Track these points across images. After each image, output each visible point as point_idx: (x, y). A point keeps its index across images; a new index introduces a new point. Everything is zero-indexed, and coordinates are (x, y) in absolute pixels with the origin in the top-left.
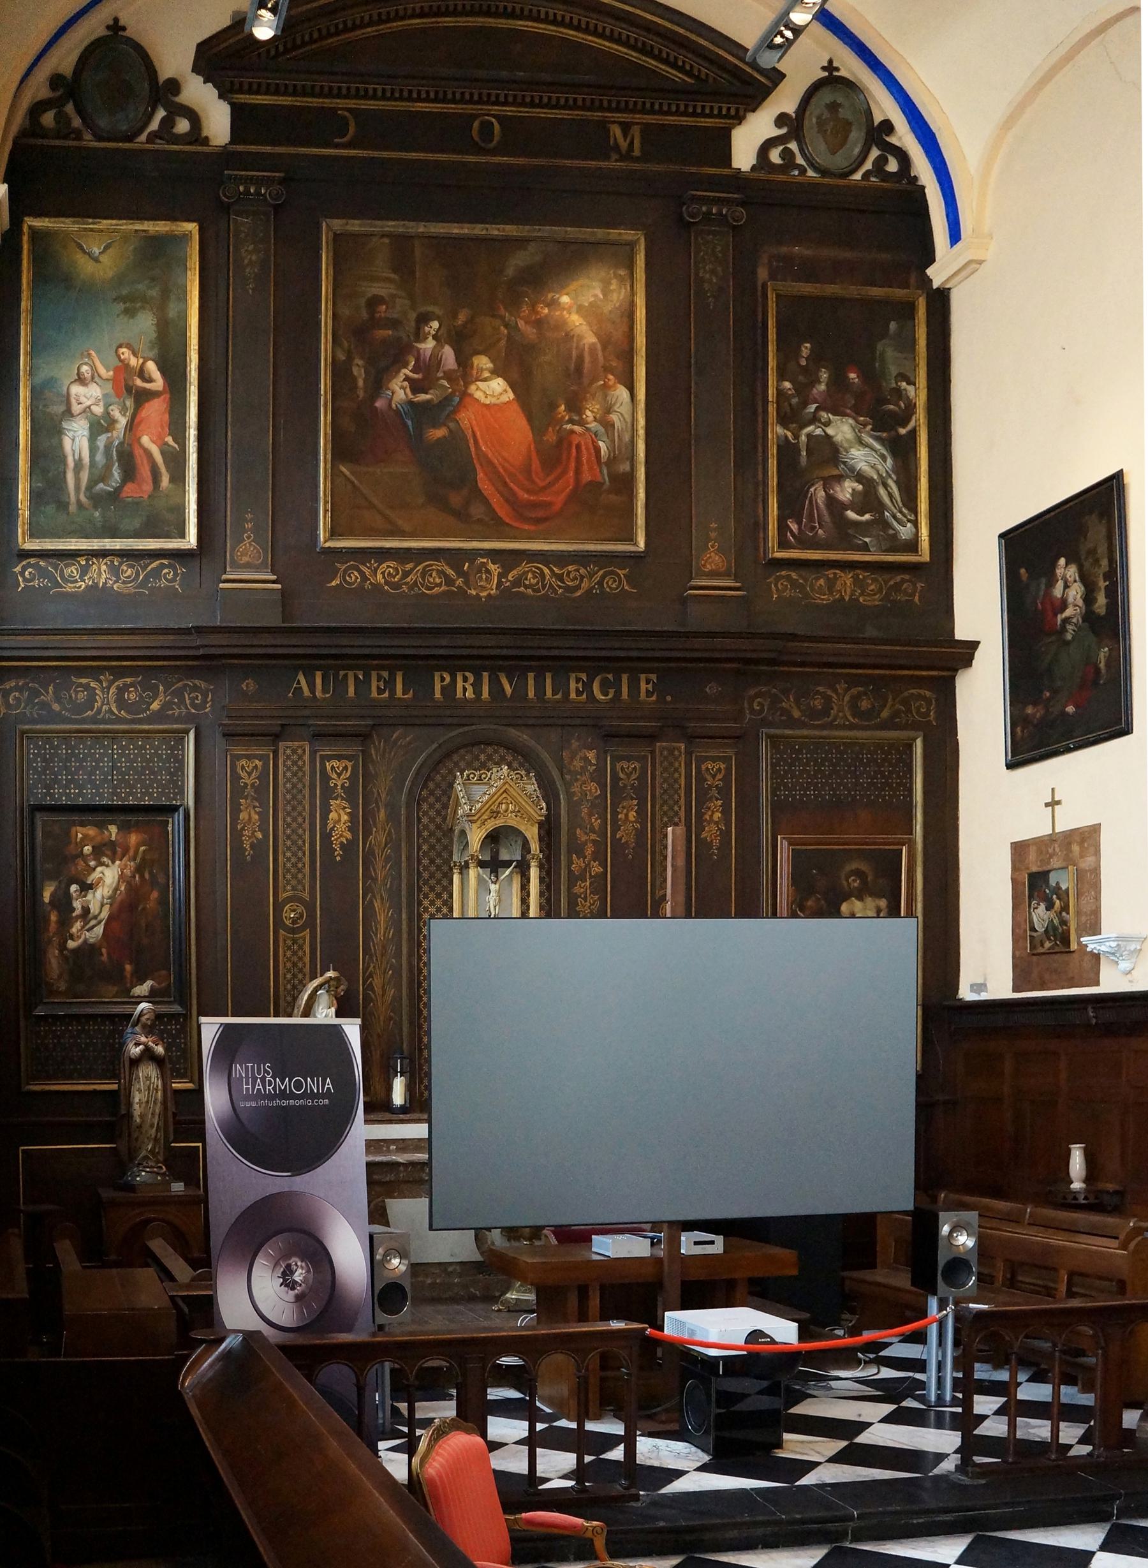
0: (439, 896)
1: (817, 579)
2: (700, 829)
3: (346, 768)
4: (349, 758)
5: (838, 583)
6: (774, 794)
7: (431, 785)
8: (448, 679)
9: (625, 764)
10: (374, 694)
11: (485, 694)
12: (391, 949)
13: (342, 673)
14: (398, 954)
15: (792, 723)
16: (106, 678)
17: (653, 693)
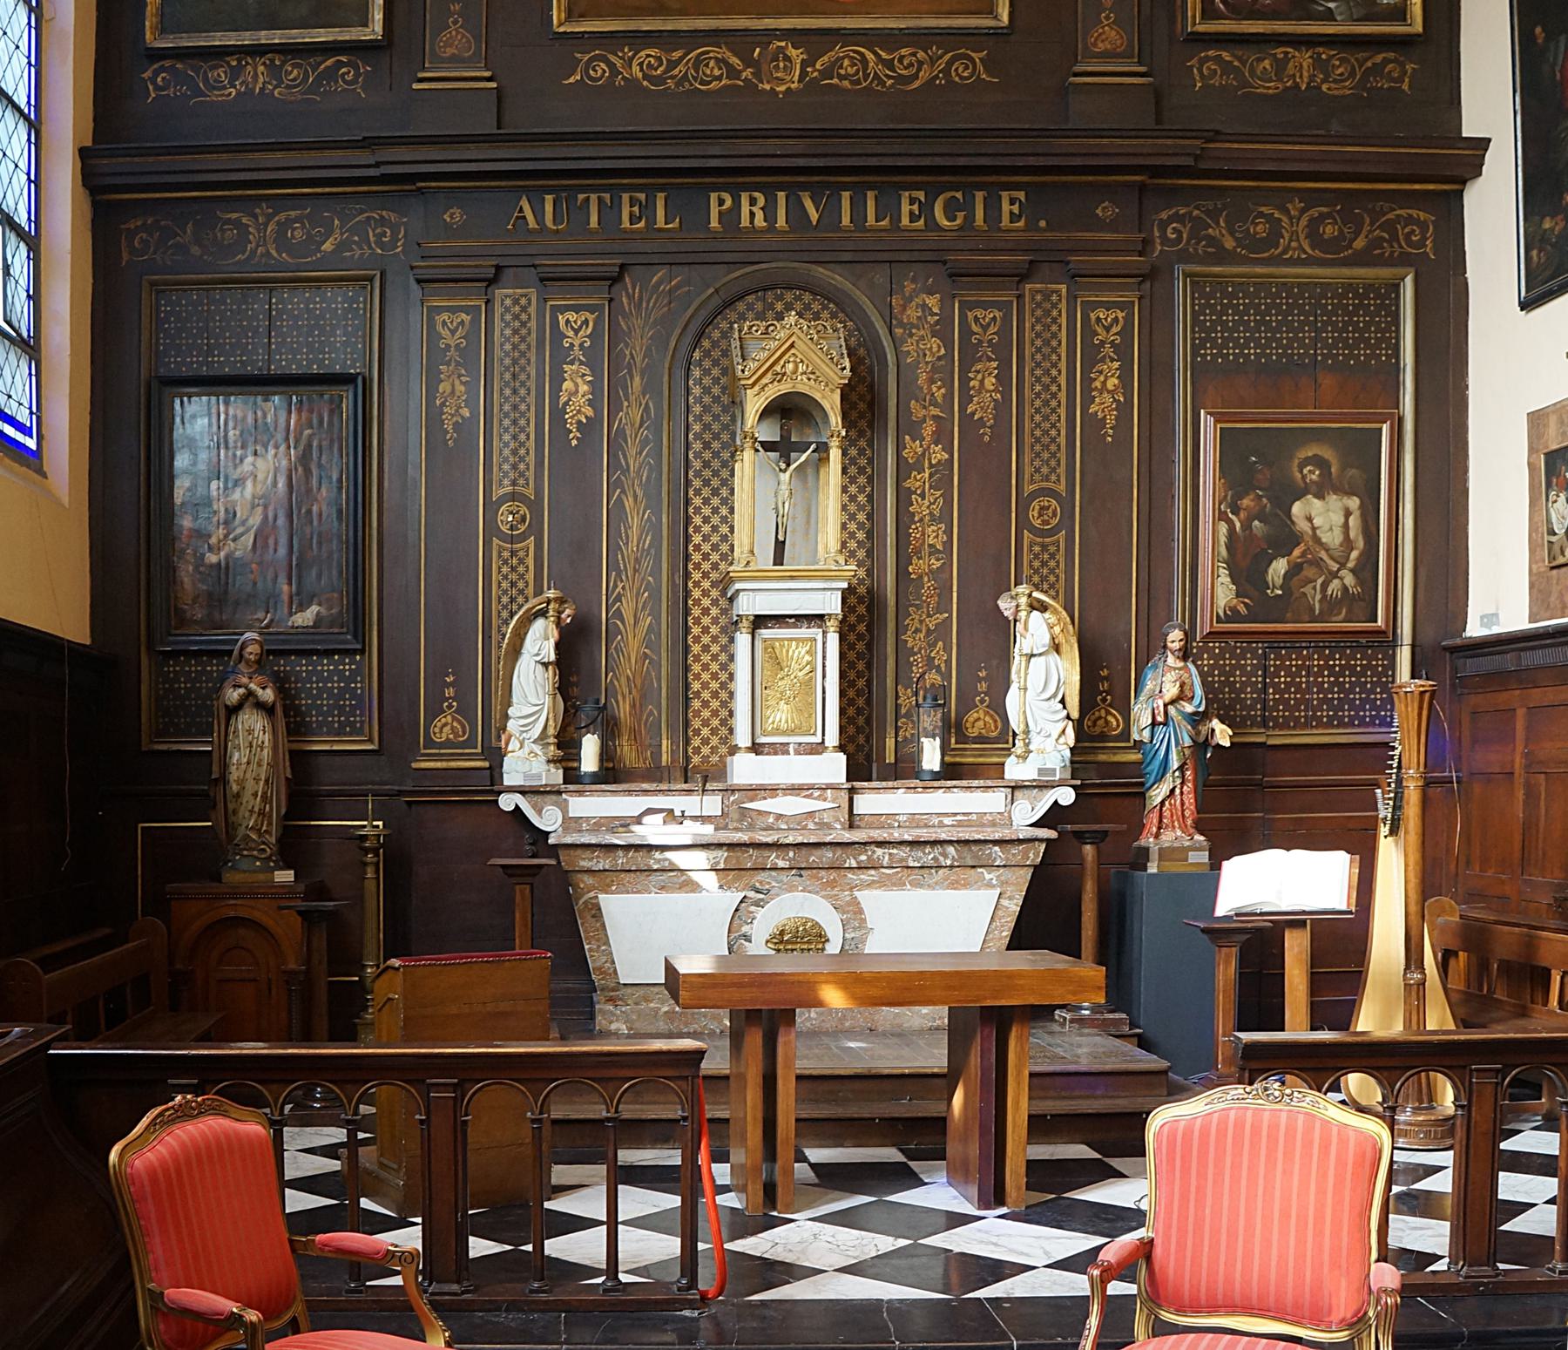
0: (715, 492)
1: (1260, 60)
2: (1088, 400)
3: (586, 322)
4: (591, 309)
5: (1291, 65)
6: (1194, 355)
7: (706, 343)
8: (728, 203)
9: (979, 313)
10: (626, 224)
11: (781, 221)
12: (647, 564)
13: (581, 197)
14: (656, 572)
15: (1222, 256)
16: (262, 210)
17: (1020, 216)
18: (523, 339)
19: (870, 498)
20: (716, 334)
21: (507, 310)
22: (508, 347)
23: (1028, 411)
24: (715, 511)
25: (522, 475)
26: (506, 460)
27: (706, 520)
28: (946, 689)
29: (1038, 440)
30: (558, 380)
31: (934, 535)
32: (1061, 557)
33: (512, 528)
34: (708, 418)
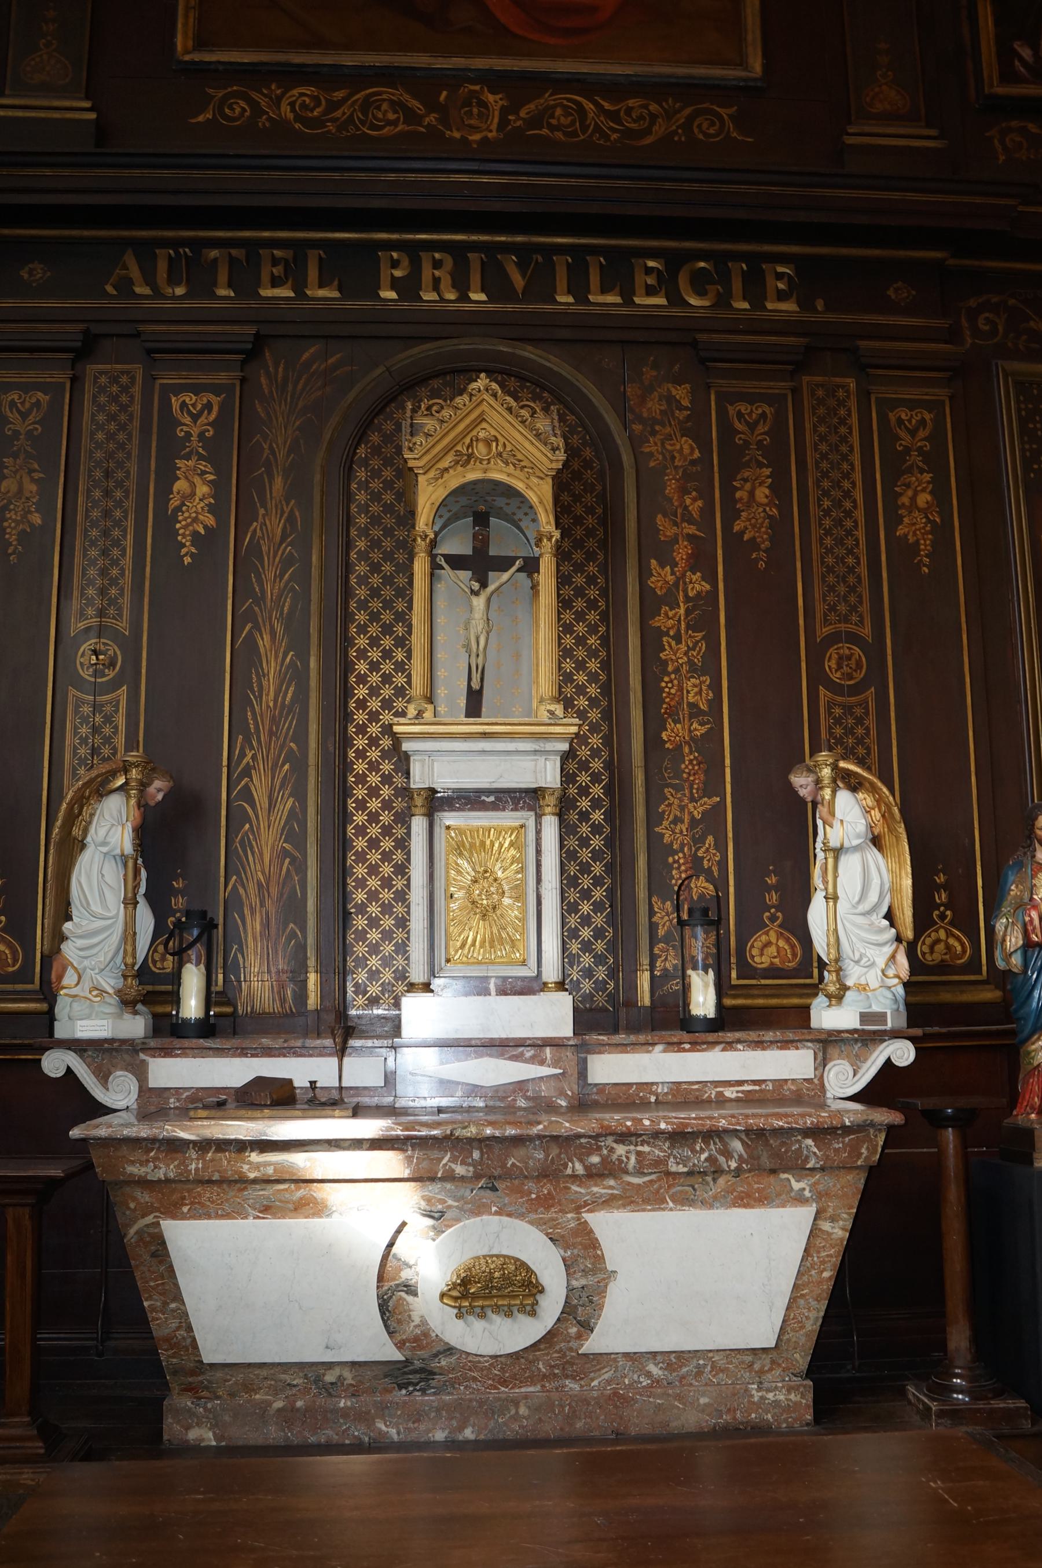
7: (375, 438)
12: (289, 725)
18: (122, 427)
19: (605, 640)
20: (389, 427)
21: (102, 389)
22: (100, 436)
23: (815, 533)
24: (387, 654)
25: (113, 602)
26: (91, 582)
27: (374, 667)
28: (720, 901)
29: (830, 570)
30: (167, 477)
31: (695, 691)
32: (871, 722)
33: (95, 674)
34: (376, 533)
